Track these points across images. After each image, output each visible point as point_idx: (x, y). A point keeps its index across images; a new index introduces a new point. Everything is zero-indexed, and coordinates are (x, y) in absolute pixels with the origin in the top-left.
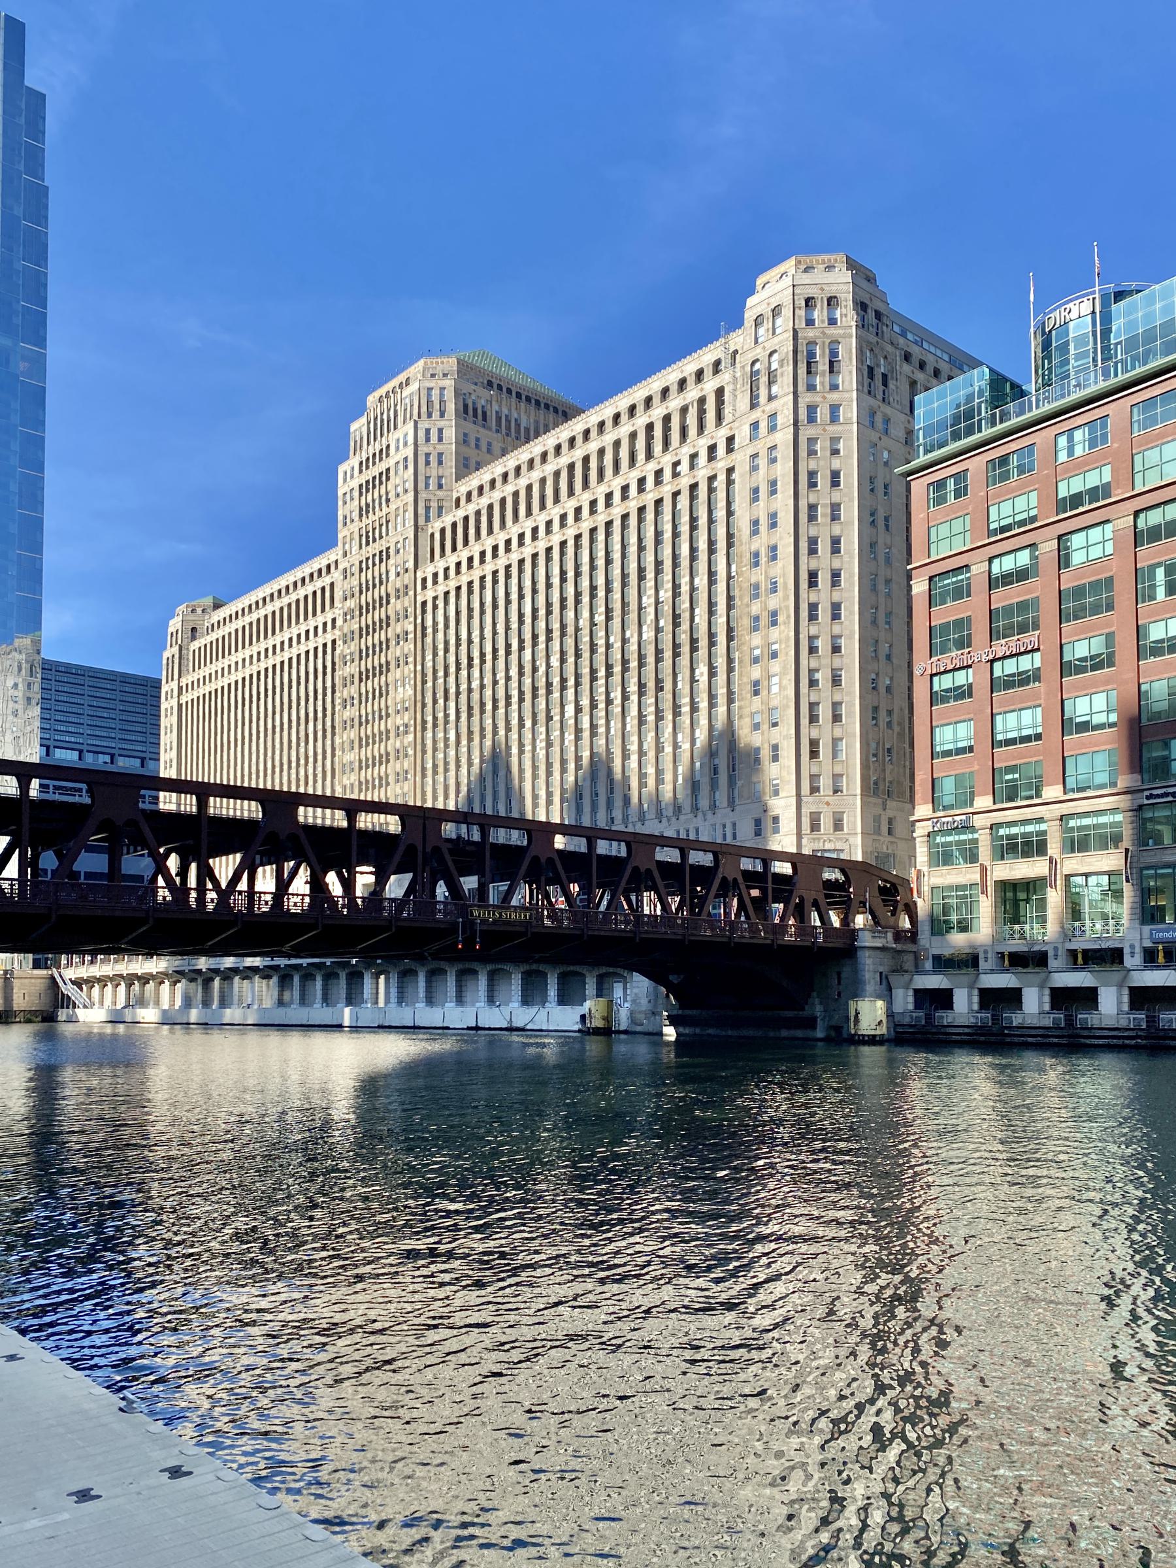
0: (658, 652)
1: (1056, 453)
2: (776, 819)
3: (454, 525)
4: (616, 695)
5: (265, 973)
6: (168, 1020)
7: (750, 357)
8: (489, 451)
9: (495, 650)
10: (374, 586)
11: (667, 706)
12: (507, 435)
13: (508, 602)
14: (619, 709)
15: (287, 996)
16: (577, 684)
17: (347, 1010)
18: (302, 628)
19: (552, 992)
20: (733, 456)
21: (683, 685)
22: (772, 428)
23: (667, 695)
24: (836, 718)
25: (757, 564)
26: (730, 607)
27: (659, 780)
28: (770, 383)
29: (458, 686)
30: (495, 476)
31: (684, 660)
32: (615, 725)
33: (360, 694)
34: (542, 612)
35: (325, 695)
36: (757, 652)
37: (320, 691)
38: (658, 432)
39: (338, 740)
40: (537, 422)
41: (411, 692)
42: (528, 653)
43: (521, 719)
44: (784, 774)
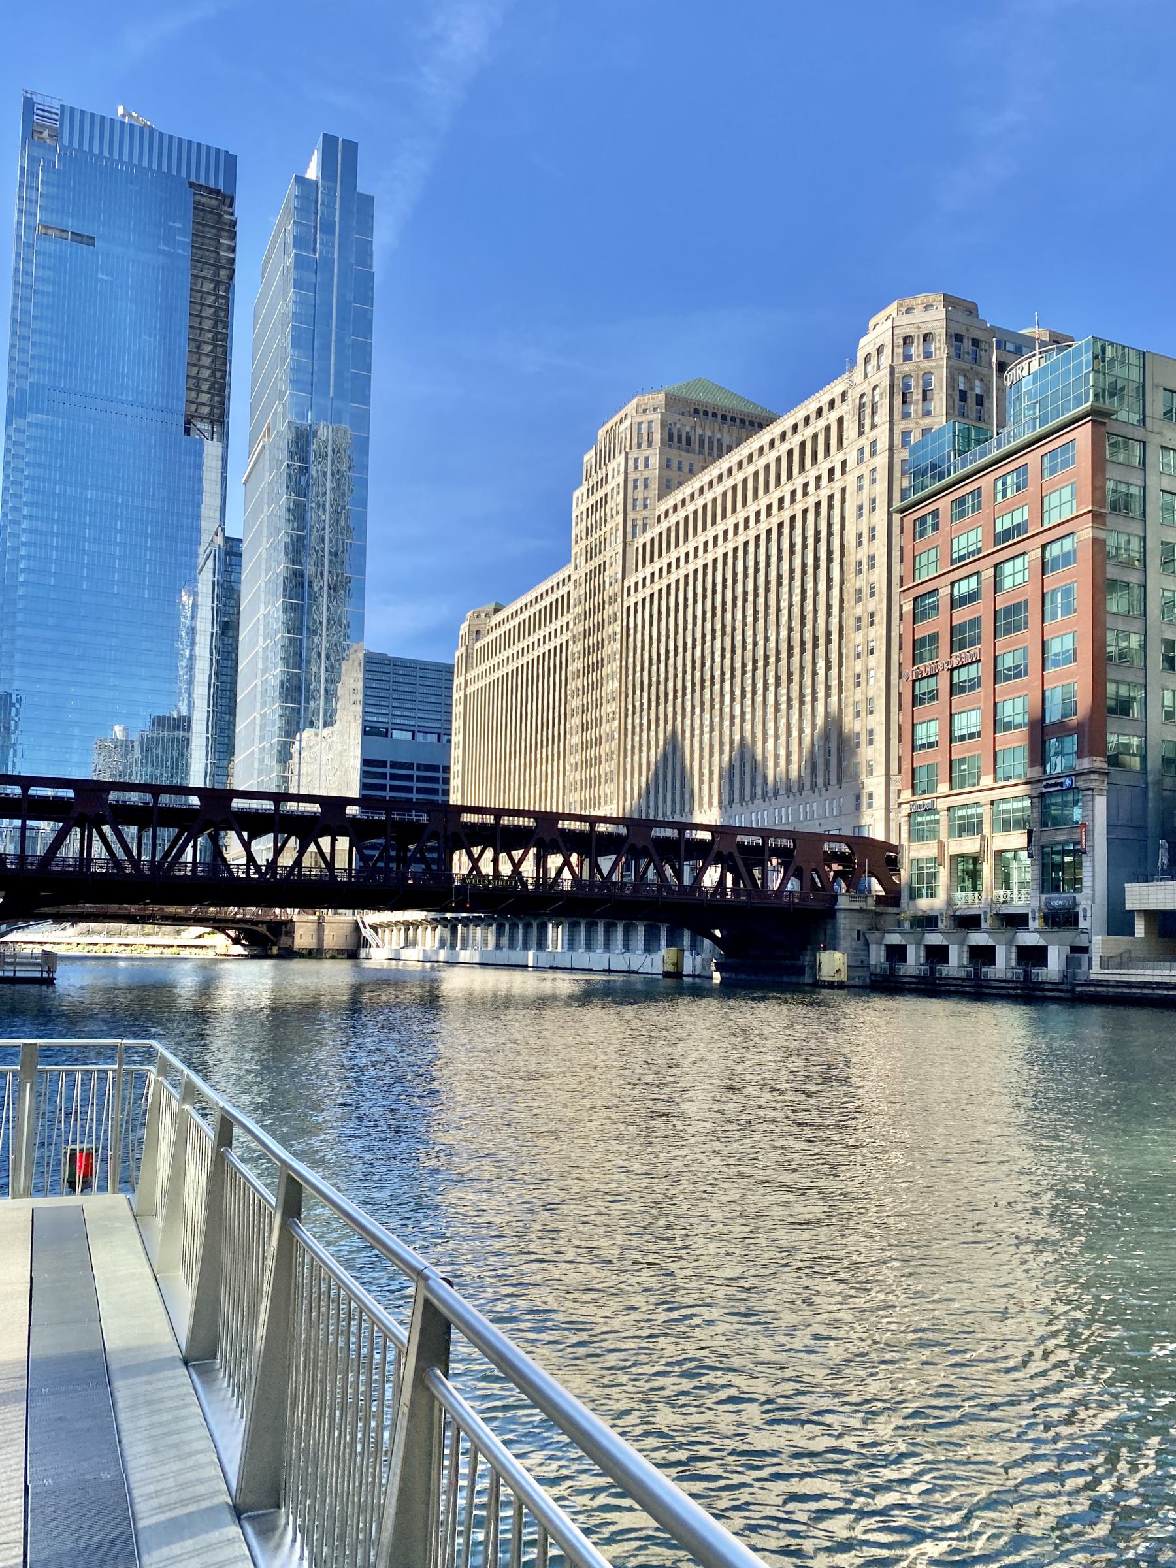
0: (790, 648)
2: (870, 796)
3: (652, 540)
11: (795, 695)
19: (663, 942)
22: (873, 453)
23: (795, 687)
25: (860, 572)
28: (873, 413)
36: (860, 649)
39: (568, 726)
41: (617, 684)
44: (877, 755)
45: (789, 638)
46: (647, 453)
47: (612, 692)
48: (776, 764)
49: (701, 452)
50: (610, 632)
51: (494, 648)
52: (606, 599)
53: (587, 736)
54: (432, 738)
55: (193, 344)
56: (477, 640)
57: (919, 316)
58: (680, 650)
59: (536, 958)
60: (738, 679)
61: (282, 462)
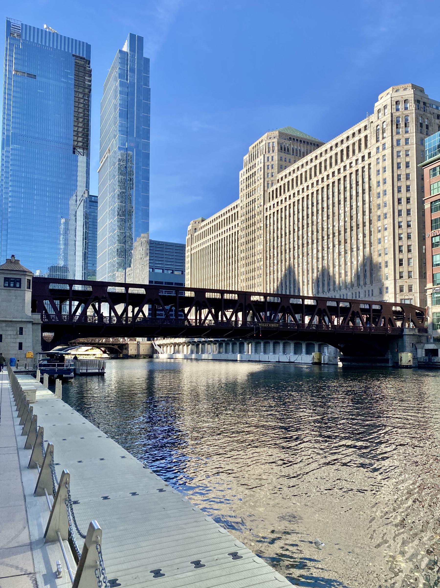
0: (345, 230)
2: (387, 288)
3: (277, 189)
4: (331, 245)
5: (215, 343)
6: (186, 358)
8: (290, 162)
9: (290, 232)
10: (251, 212)
12: (296, 155)
13: (294, 214)
14: (332, 250)
15: (221, 350)
16: (317, 242)
17: (239, 355)
18: (228, 227)
20: (370, 159)
21: (354, 241)
22: (384, 149)
23: (348, 245)
24: (409, 251)
25: (379, 197)
26: (370, 212)
27: (346, 275)
30: (291, 171)
31: (354, 232)
32: (330, 256)
33: (246, 249)
34: (305, 217)
35: (235, 249)
36: (380, 228)
37: (234, 248)
38: (345, 152)
39: (239, 264)
40: (307, 150)
41: (262, 247)
42: (300, 232)
43: (298, 255)
44: (390, 272)
49: (293, 155)
50: (258, 226)
52: (256, 213)
53: (248, 268)
54: (170, 272)
55: (76, 118)
57: (401, 93)
58: (292, 232)
59: (241, 357)
60: (320, 243)
61: (115, 163)
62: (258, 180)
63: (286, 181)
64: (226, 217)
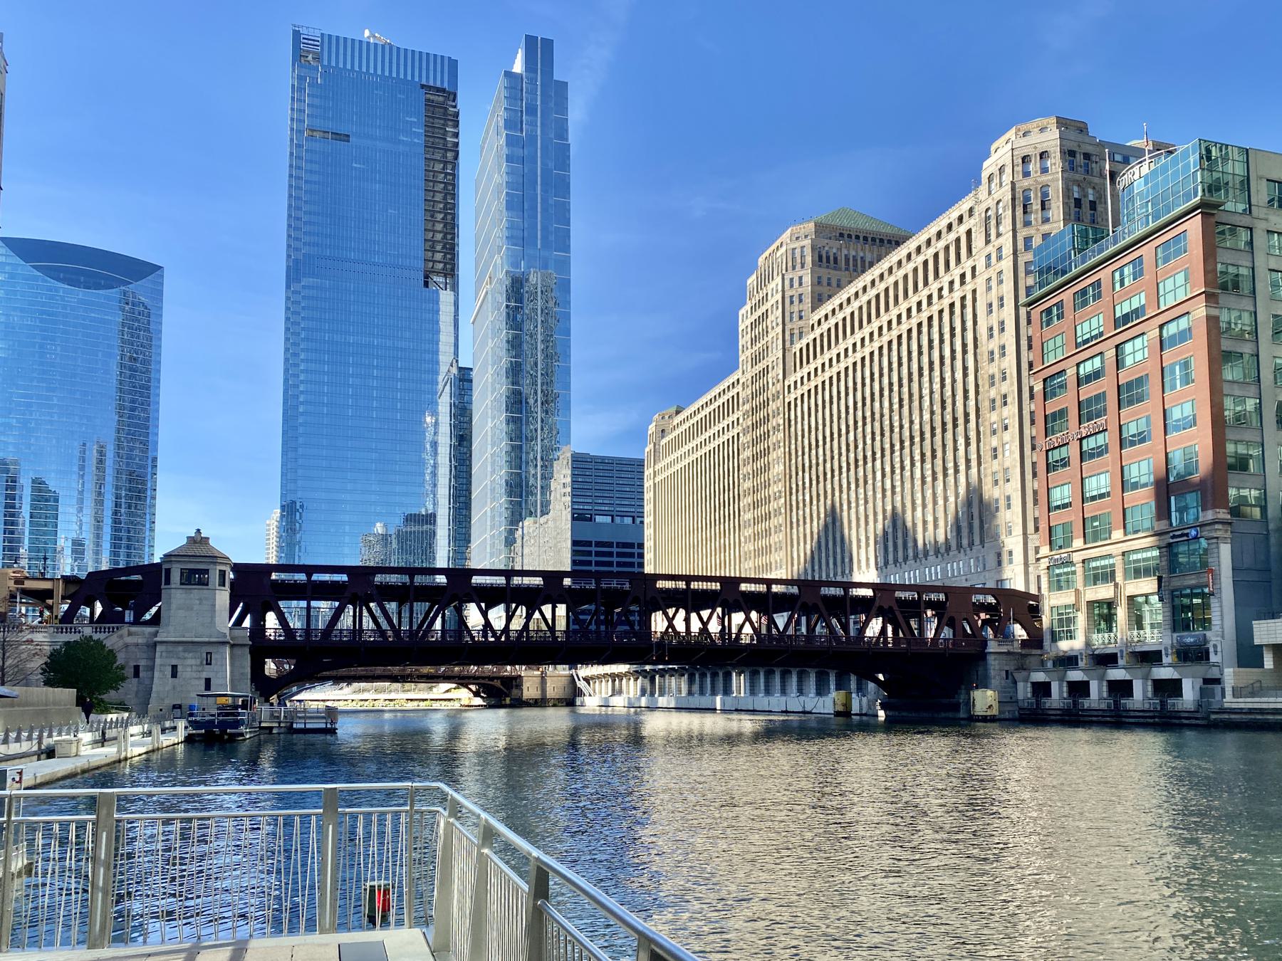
0: (933, 429)
1: (1113, 284)
2: (1010, 553)
3: (808, 345)
4: (907, 463)
7: (983, 207)
11: (939, 469)
19: (832, 687)
22: (1000, 258)
23: (939, 461)
25: (992, 360)
26: (977, 393)
28: (998, 224)
29: (810, 461)
36: (995, 426)
39: (741, 505)
41: (782, 468)
44: (1015, 518)
45: (931, 420)
46: (800, 273)
47: (778, 474)
48: (925, 529)
49: (847, 269)
50: (774, 424)
51: (678, 442)
52: (770, 397)
53: (758, 512)
54: (628, 521)
56: (663, 437)
58: (836, 436)
59: (723, 703)
62: (773, 328)
63: (825, 326)
64: (717, 404)
